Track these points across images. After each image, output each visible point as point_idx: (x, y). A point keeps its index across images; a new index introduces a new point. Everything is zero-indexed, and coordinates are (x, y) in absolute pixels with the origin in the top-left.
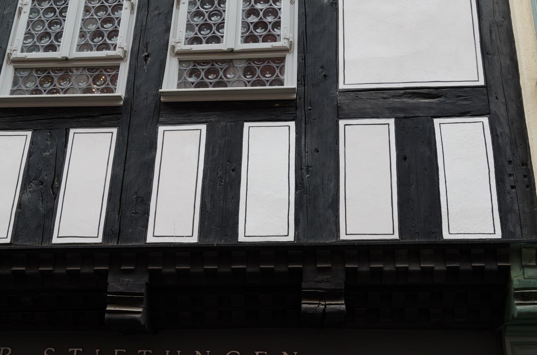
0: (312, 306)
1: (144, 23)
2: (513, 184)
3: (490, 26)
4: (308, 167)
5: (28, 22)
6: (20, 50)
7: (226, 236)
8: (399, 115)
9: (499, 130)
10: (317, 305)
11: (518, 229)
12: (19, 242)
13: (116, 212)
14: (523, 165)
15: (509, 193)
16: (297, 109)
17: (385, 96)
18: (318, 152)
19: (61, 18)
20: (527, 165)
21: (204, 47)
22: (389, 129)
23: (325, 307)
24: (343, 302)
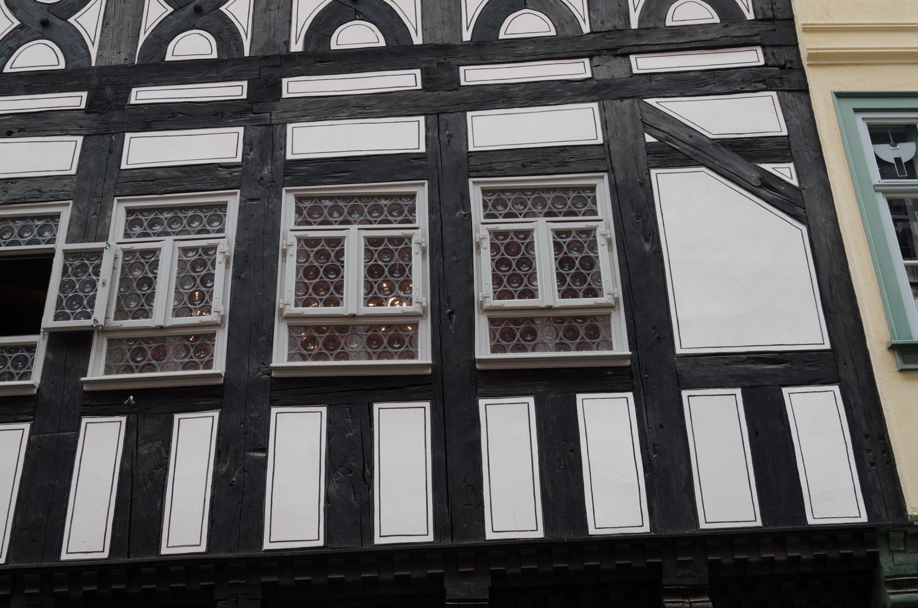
0: (677, 605)
1: (442, 272)
2: (873, 461)
3: (829, 280)
4: (654, 445)
5: (297, 267)
6: (293, 304)
7: (575, 528)
8: (744, 383)
9: (852, 400)
10: (681, 604)
11: (883, 511)
13: (445, 505)
14: (880, 439)
15: (869, 471)
16: (632, 377)
17: (727, 362)
18: (663, 427)
19: (338, 264)
20: (884, 439)
21: (516, 303)
22: (736, 400)
23: (691, 605)
24: (708, 599)
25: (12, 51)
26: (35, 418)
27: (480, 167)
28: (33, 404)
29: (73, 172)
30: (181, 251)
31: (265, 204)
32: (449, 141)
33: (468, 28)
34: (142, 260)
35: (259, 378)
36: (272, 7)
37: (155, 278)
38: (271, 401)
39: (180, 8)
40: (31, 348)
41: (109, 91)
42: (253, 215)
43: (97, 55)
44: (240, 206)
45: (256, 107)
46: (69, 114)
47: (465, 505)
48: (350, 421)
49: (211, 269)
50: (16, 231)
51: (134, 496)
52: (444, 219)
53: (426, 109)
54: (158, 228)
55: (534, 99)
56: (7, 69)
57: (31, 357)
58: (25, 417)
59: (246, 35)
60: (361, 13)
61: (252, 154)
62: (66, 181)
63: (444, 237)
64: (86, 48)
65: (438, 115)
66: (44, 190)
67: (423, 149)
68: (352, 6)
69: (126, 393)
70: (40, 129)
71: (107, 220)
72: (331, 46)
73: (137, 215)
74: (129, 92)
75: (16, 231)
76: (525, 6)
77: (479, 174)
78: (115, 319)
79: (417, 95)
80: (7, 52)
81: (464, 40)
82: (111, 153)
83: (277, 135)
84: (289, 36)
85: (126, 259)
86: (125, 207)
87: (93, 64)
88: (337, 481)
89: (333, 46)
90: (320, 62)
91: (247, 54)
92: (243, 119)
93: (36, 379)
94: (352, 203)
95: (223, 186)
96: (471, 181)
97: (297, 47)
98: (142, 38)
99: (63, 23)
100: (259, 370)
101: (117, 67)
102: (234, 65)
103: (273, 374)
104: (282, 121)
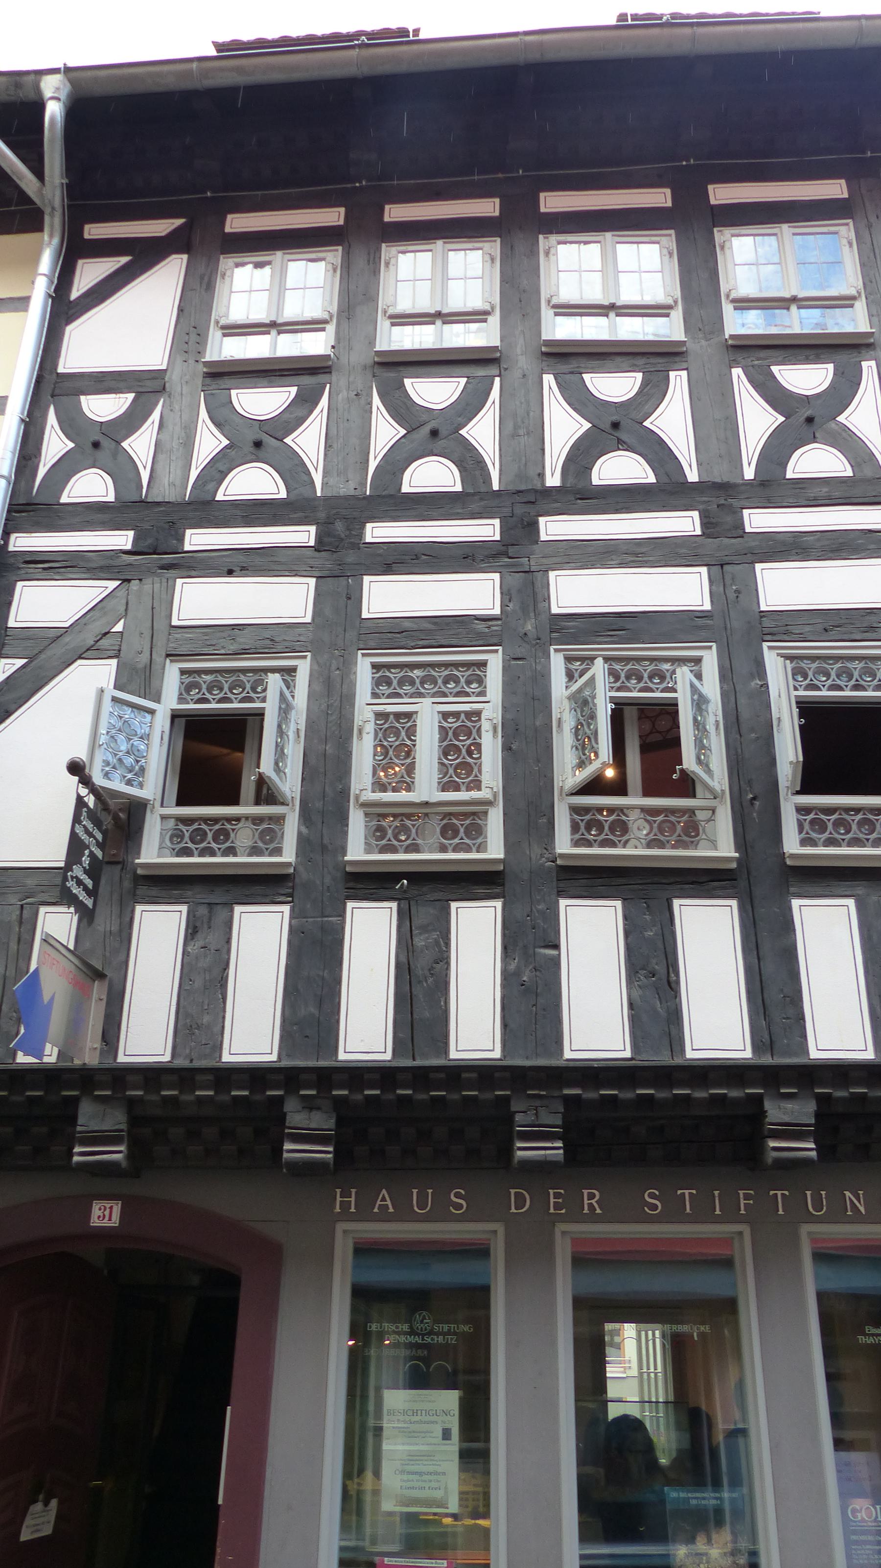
1: (739, 751)
12: (644, 1057)
13: (763, 1018)
25: (224, 475)
26: (295, 900)
27: (775, 629)
28: (291, 884)
29: (308, 619)
30: (440, 715)
31: (531, 664)
32: (737, 597)
33: (749, 464)
34: (397, 725)
35: (542, 865)
36: (521, 432)
37: (414, 745)
38: (558, 892)
39: (414, 430)
40: (280, 820)
41: (339, 527)
42: (519, 677)
43: (322, 483)
44: (503, 667)
45: (512, 551)
46: (297, 551)
47: (784, 1018)
48: (647, 917)
49: (477, 737)
50: (248, 686)
51: (414, 993)
52: (737, 690)
53: (708, 559)
54: (407, 688)
55: (832, 551)
56: (219, 497)
57: (280, 830)
58: (282, 899)
59: (494, 464)
60: (624, 443)
61: (511, 605)
62: (301, 630)
63: (739, 710)
64: (309, 473)
65: (722, 565)
66: (277, 639)
67: (707, 606)
68: (613, 433)
69: (396, 877)
70: (265, 568)
71: (352, 677)
72: (593, 480)
73: (384, 672)
74: (363, 527)
75: (248, 686)
76: (814, 440)
77: (775, 638)
78: (373, 792)
79: (696, 542)
80: (218, 476)
81: (746, 478)
82: (349, 598)
83: (538, 584)
84: (544, 467)
85: (378, 722)
86: (371, 662)
87: (319, 494)
88: (639, 986)
89: (595, 481)
90: (581, 499)
91: (496, 487)
92: (497, 564)
93: (289, 855)
94: (629, 667)
95: (481, 642)
96: (765, 645)
97: (553, 480)
98: (373, 465)
99: (278, 443)
100: (542, 856)
101: (347, 498)
102: (481, 499)
103: (559, 862)
104: (543, 568)
